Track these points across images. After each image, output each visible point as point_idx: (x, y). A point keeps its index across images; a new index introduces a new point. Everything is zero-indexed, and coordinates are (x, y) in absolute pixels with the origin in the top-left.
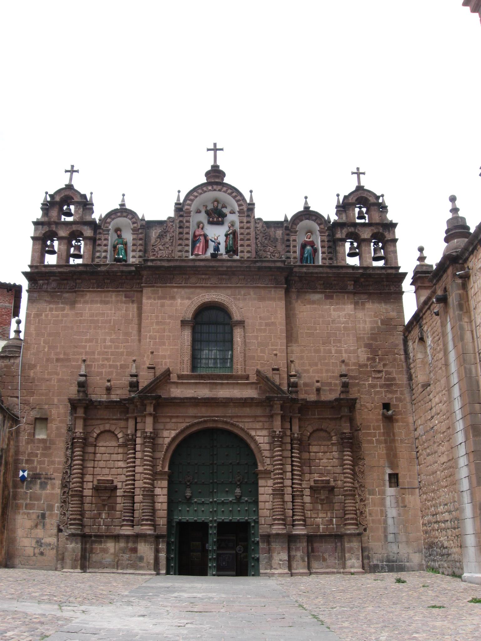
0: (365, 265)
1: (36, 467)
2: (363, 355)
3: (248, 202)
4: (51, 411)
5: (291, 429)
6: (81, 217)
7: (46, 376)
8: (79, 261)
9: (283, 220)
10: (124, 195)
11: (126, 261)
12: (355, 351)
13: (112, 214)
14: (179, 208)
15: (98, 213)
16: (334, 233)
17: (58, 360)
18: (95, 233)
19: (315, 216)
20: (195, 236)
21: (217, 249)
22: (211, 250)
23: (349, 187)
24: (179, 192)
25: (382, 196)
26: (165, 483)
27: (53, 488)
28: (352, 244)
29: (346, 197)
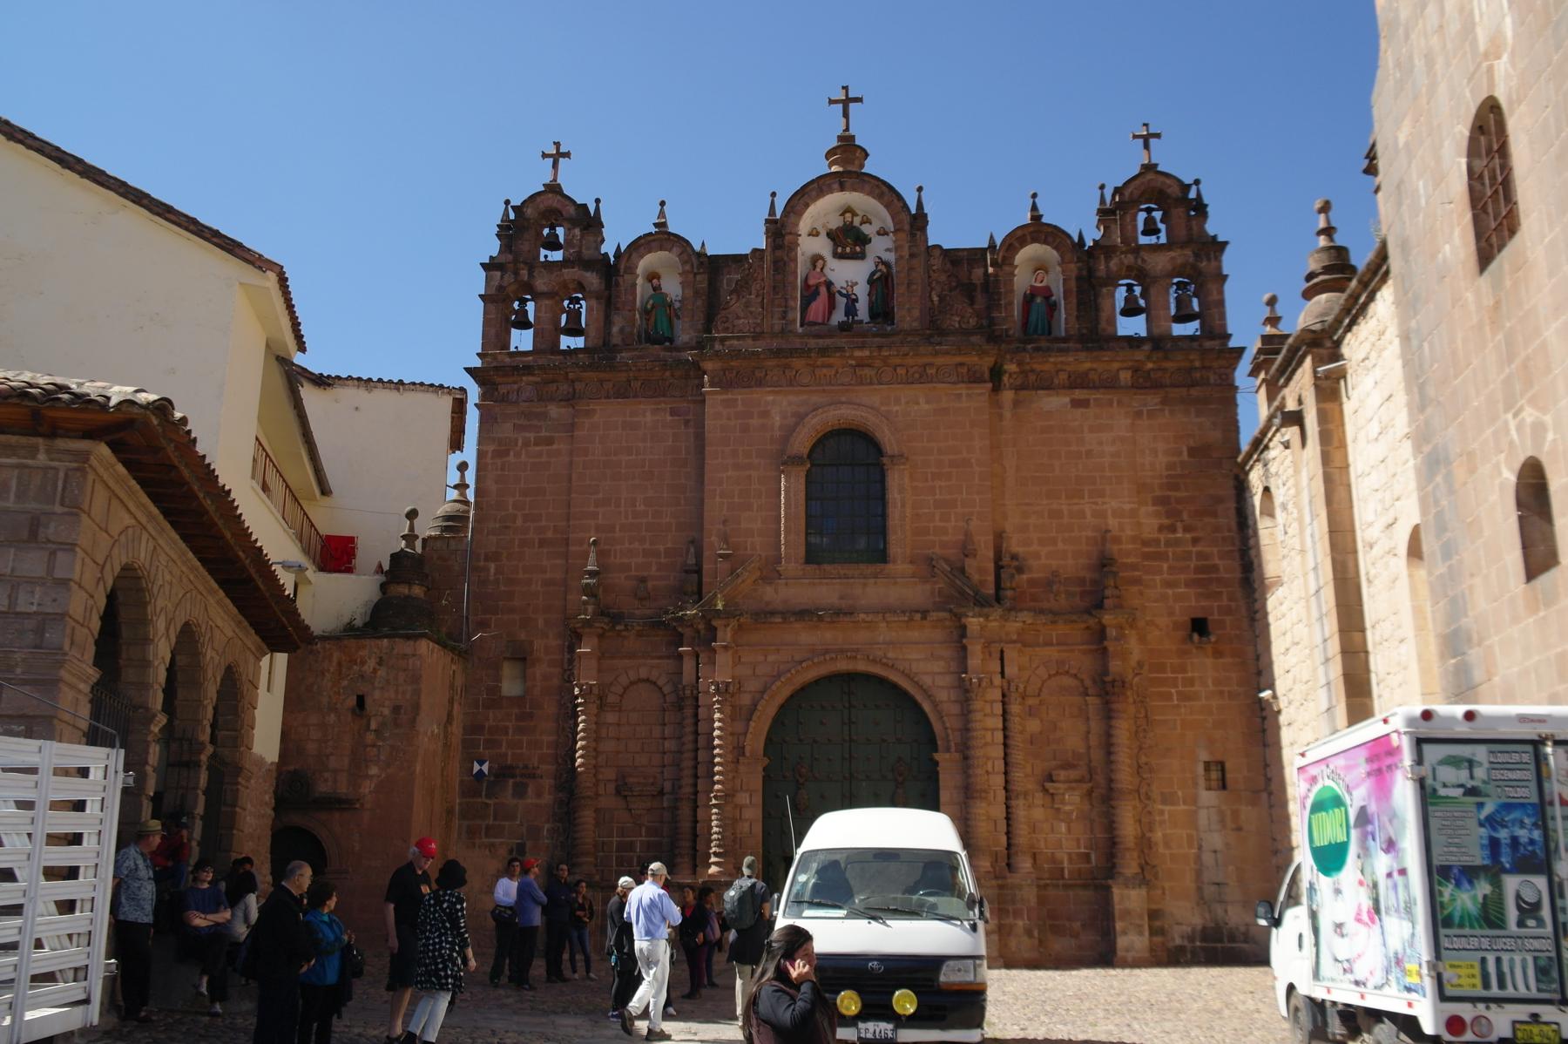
0: (1156, 331)
1: (506, 755)
2: (1149, 521)
3: (913, 211)
4: (531, 643)
5: (1002, 673)
6: (579, 253)
7: (521, 576)
8: (579, 342)
9: (986, 245)
10: (663, 204)
11: (671, 340)
12: (1133, 513)
13: (641, 245)
15: (615, 238)
16: (1089, 267)
17: (542, 543)
18: (609, 286)
20: (806, 285)
21: (851, 309)
22: (839, 316)
23: (1123, 167)
24: (774, 194)
25: (1197, 182)
26: (757, 782)
27: (539, 795)
28: (1130, 288)
29: (1117, 190)
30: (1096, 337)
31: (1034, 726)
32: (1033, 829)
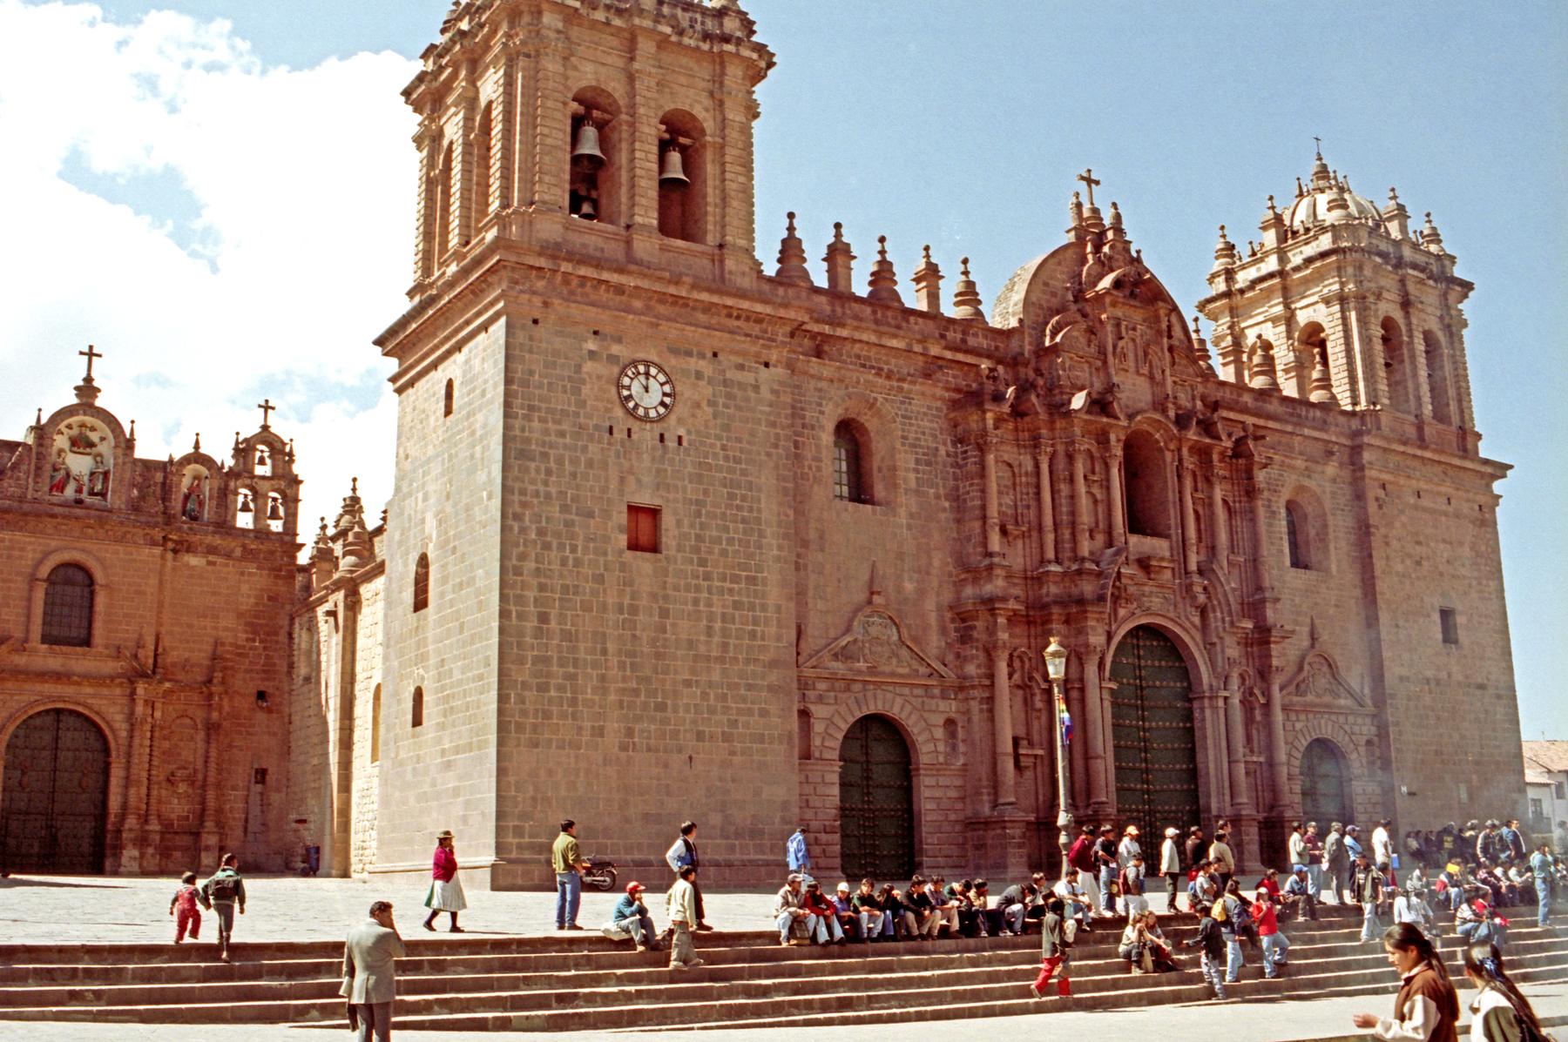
14: (39, 430)
19: (206, 461)
23: (251, 429)
29: (246, 440)
30: (224, 526)
31: (166, 744)
32: (160, 802)
